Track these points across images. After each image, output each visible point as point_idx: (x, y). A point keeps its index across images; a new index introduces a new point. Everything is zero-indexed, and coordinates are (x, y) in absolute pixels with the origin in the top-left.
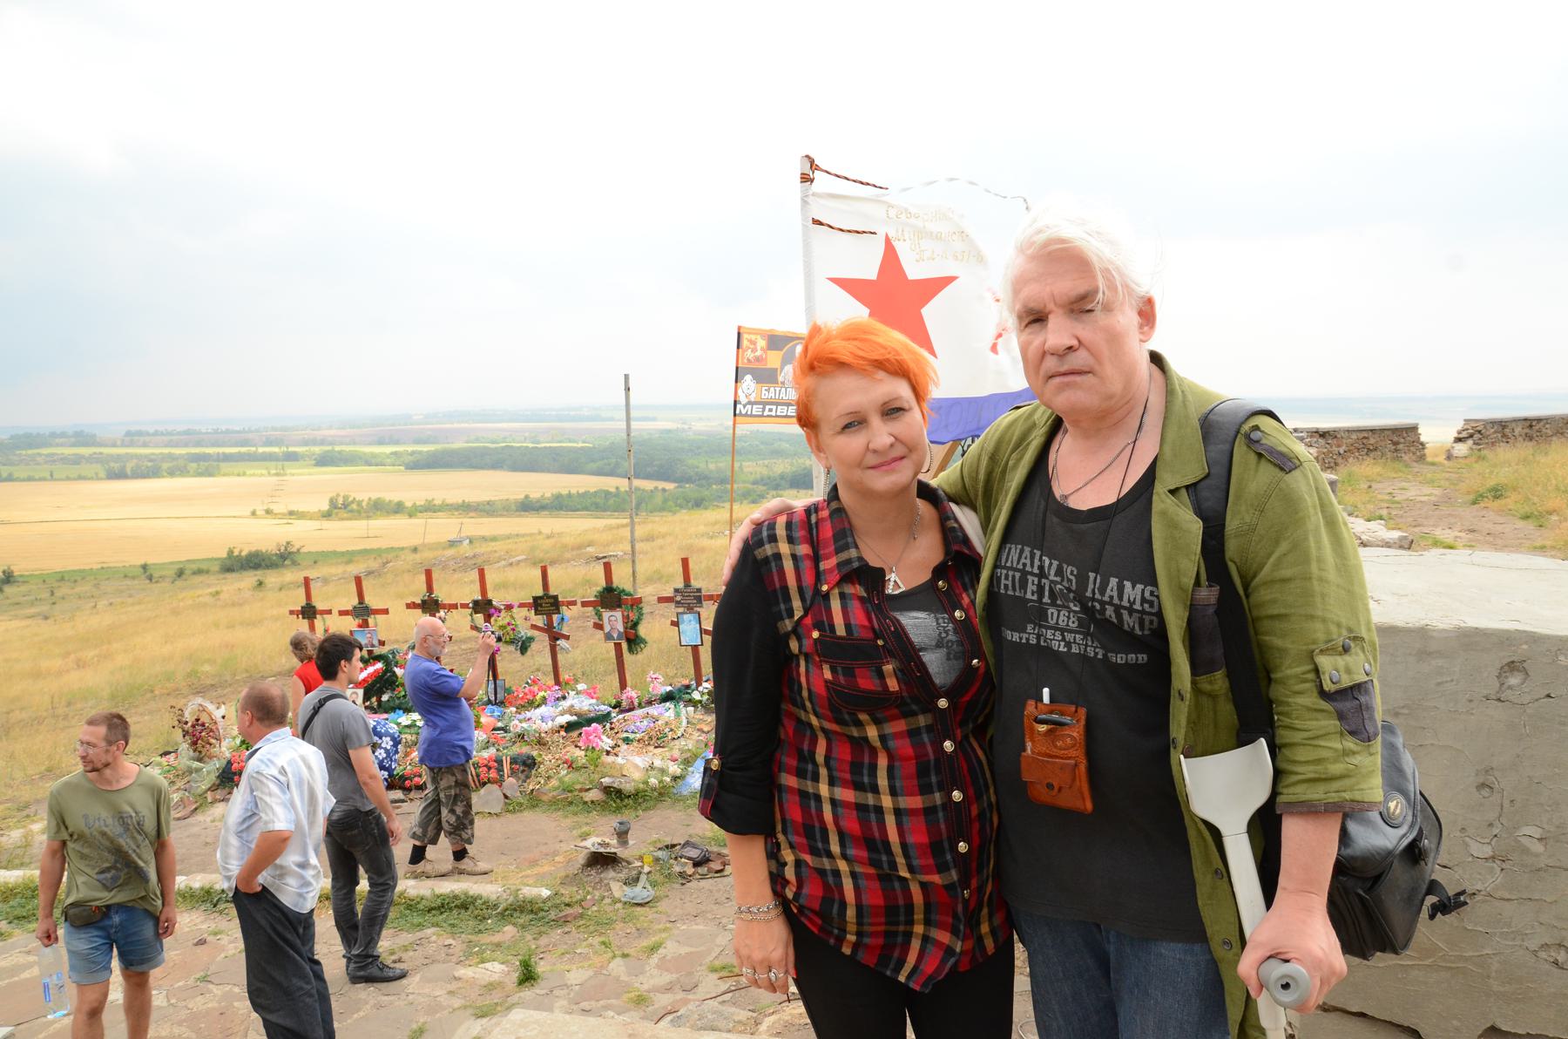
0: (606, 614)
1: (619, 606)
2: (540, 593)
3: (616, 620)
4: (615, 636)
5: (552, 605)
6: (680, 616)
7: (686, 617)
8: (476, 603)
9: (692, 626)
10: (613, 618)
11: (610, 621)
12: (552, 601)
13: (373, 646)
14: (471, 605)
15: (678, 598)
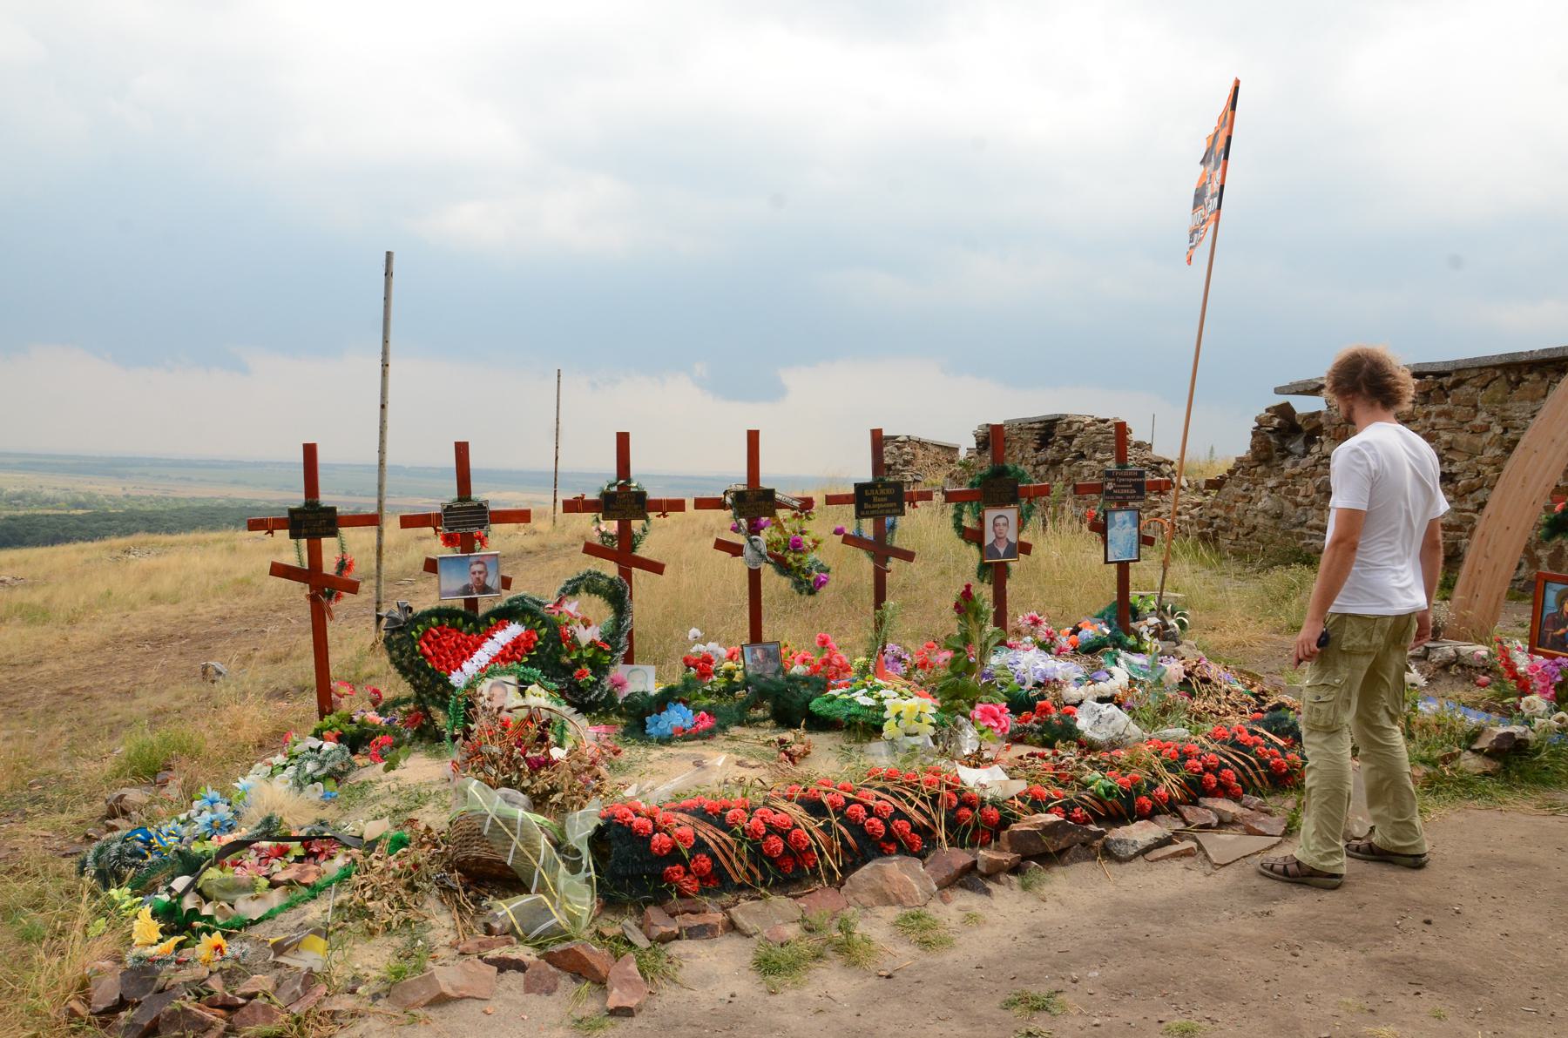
0: (990, 515)
1: (1014, 500)
2: (866, 476)
3: (1006, 524)
4: (1002, 550)
5: (890, 499)
6: (1109, 516)
7: (1120, 516)
8: (739, 497)
9: (1127, 531)
10: (1001, 521)
11: (995, 525)
12: (890, 491)
13: (485, 589)
14: (728, 500)
15: (1110, 486)
